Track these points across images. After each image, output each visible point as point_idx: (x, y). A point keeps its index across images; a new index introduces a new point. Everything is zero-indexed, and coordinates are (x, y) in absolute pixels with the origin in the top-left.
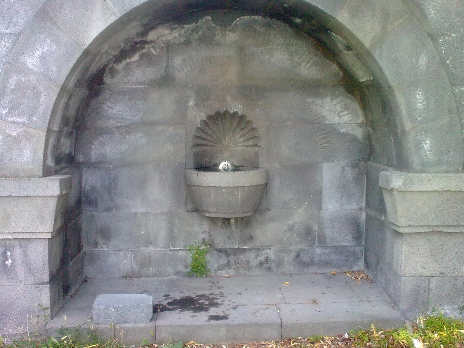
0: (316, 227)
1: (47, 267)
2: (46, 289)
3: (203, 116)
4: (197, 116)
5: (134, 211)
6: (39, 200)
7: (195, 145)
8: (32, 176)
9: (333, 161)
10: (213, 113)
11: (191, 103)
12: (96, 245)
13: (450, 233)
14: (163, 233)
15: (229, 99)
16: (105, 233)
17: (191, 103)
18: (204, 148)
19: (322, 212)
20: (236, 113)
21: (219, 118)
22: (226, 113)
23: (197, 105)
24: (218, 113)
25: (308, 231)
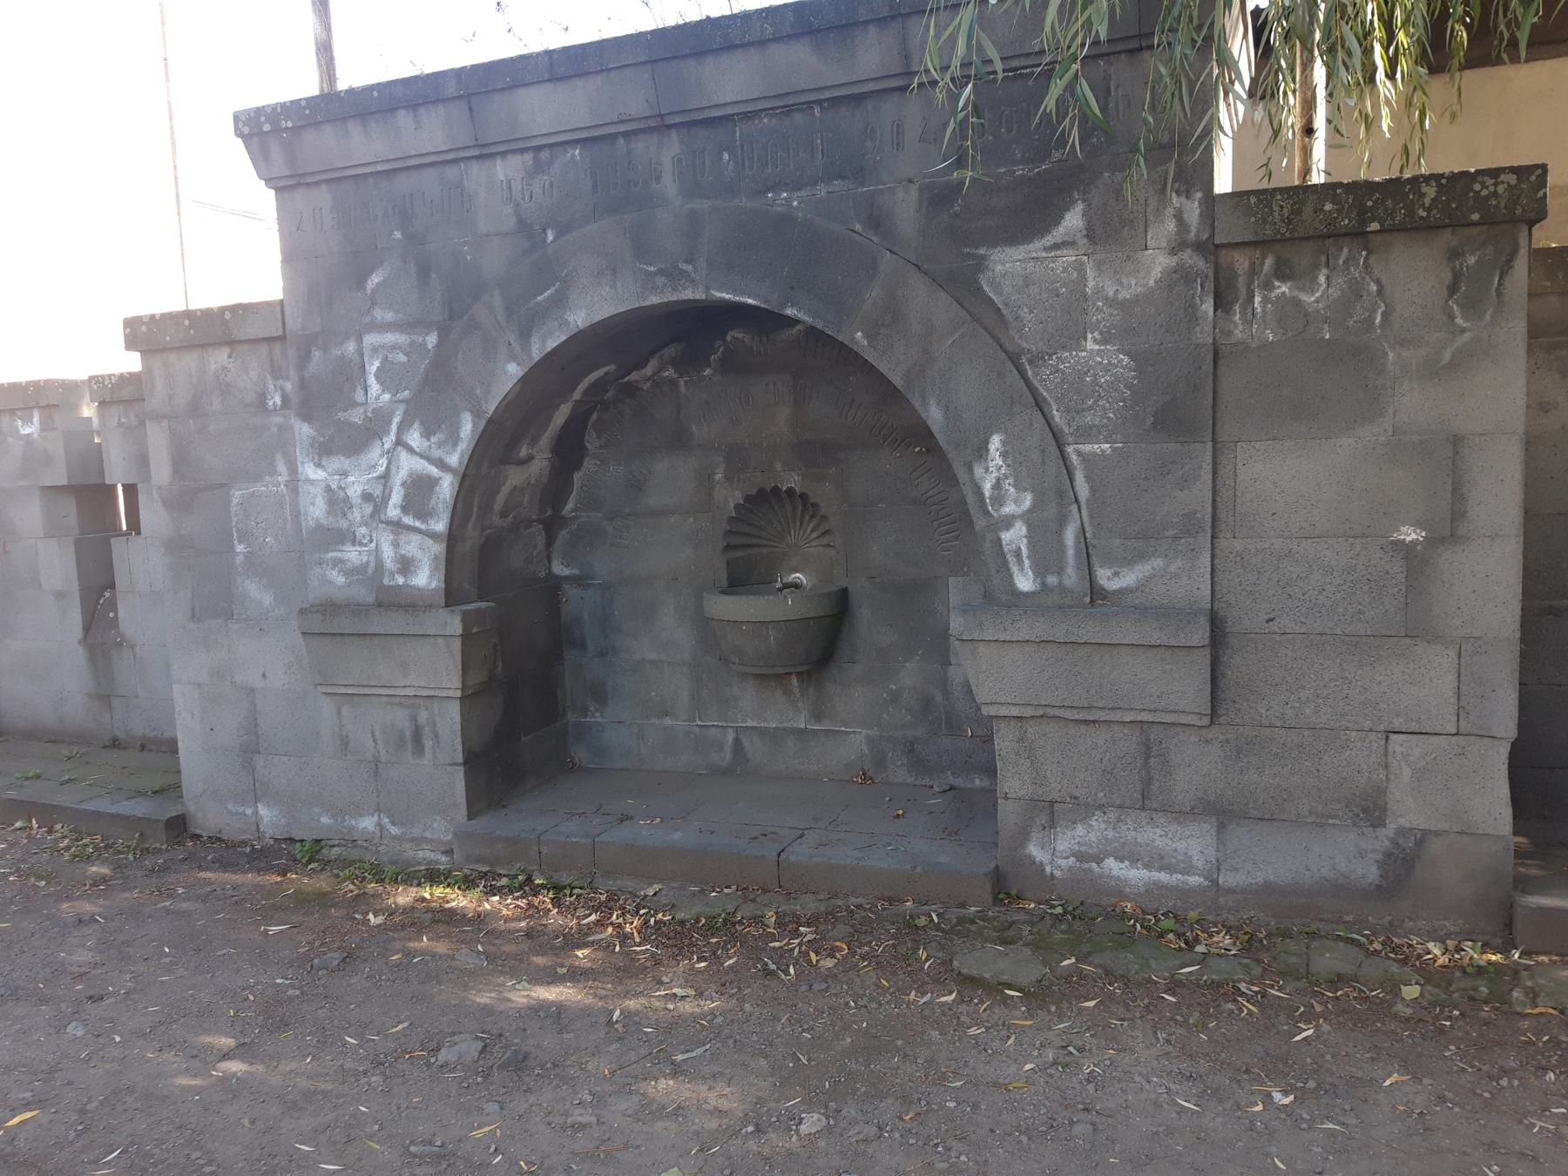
0: (939, 698)
1: (459, 740)
2: (460, 773)
3: (738, 497)
4: (730, 497)
5: (638, 657)
6: (440, 640)
7: (728, 547)
8: (431, 606)
9: (966, 574)
10: (753, 492)
11: (719, 477)
12: (585, 711)
13: (1086, 722)
14: (685, 697)
15: (778, 466)
16: (599, 694)
17: (719, 477)
18: (750, 551)
19: (952, 671)
20: (790, 491)
21: (765, 499)
22: (775, 490)
23: (728, 479)
24: (761, 492)
25: (927, 704)
